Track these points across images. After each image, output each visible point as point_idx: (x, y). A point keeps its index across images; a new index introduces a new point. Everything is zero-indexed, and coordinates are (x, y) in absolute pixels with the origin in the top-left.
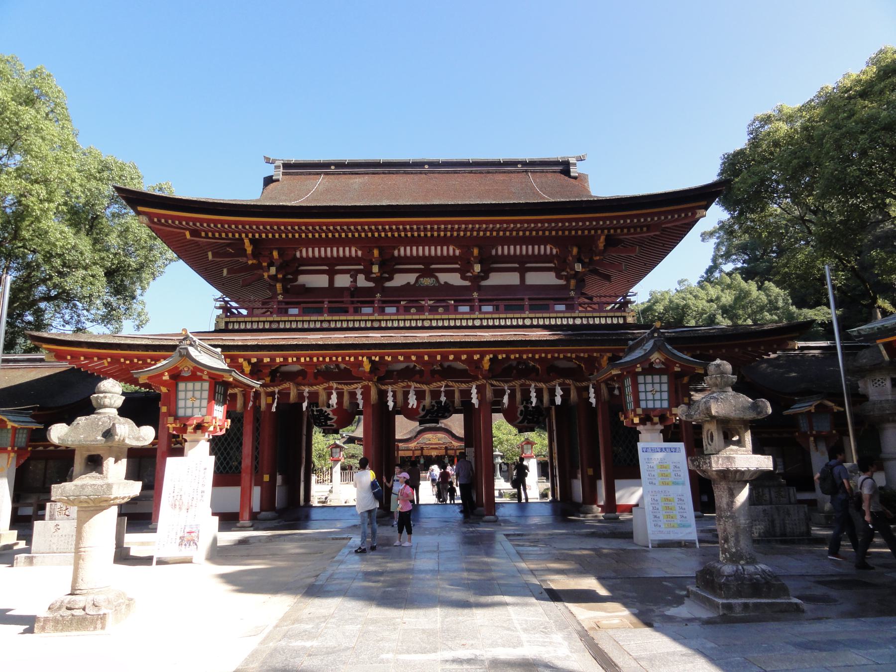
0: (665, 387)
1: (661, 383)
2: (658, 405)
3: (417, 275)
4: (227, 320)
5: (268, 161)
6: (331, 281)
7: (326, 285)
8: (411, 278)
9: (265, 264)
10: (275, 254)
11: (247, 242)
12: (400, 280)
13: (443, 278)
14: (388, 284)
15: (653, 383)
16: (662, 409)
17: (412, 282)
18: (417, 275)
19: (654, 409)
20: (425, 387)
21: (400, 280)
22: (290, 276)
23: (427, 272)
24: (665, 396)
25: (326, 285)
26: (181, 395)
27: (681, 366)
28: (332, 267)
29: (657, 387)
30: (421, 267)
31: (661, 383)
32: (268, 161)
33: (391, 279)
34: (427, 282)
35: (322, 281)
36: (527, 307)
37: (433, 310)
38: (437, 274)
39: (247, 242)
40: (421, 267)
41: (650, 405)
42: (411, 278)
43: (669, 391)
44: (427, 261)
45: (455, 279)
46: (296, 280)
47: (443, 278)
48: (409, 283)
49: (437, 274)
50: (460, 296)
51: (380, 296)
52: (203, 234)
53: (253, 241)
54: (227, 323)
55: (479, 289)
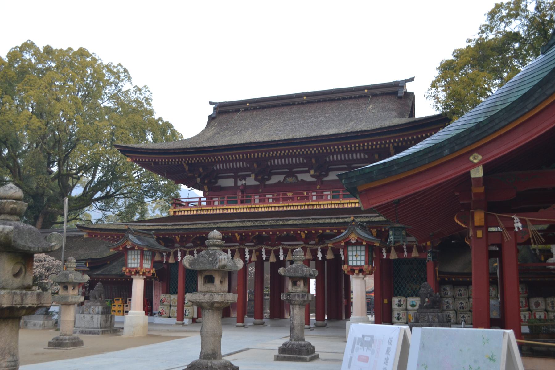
0: (363, 253)
1: (361, 251)
2: (359, 263)
3: (285, 176)
4: (175, 210)
5: (211, 103)
6: (236, 183)
7: (233, 185)
8: (281, 178)
9: (196, 175)
10: (201, 169)
11: (185, 165)
12: (274, 180)
13: (301, 177)
14: (268, 183)
15: (357, 251)
16: (361, 266)
17: (282, 180)
18: (285, 176)
19: (357, 266)
20: (270, 248)
21: (274, 180)
22: (213, 181)
23: (290, 174)
24: (363, 258)
25: (233, 185)
26: (129, 257)
27: (366, 241)
28: (237, 175)
29: (359, 253)
30: (287, 170)
31: (361, 251)
32: (211, 103)
33: (269, 179)
34: (291, 180)
35: (229, 182)
36: (341, 196)
37: (292, 199)
38: (297, 175)
39: (185, 165)
40: (287, 170)
41: (355, 263)
42: (281, 178)
43: (366, 256)
44: (290, 167)
45: (307, 177)
46: (216, 182)
47: (301, 177)
48: (280, 181)
49: (297, 175)
50: (309, 186)
51: (262, 190)
52: (160, 163)
53: (187, 164)
54: (175, 212)
55: (322, 182)
